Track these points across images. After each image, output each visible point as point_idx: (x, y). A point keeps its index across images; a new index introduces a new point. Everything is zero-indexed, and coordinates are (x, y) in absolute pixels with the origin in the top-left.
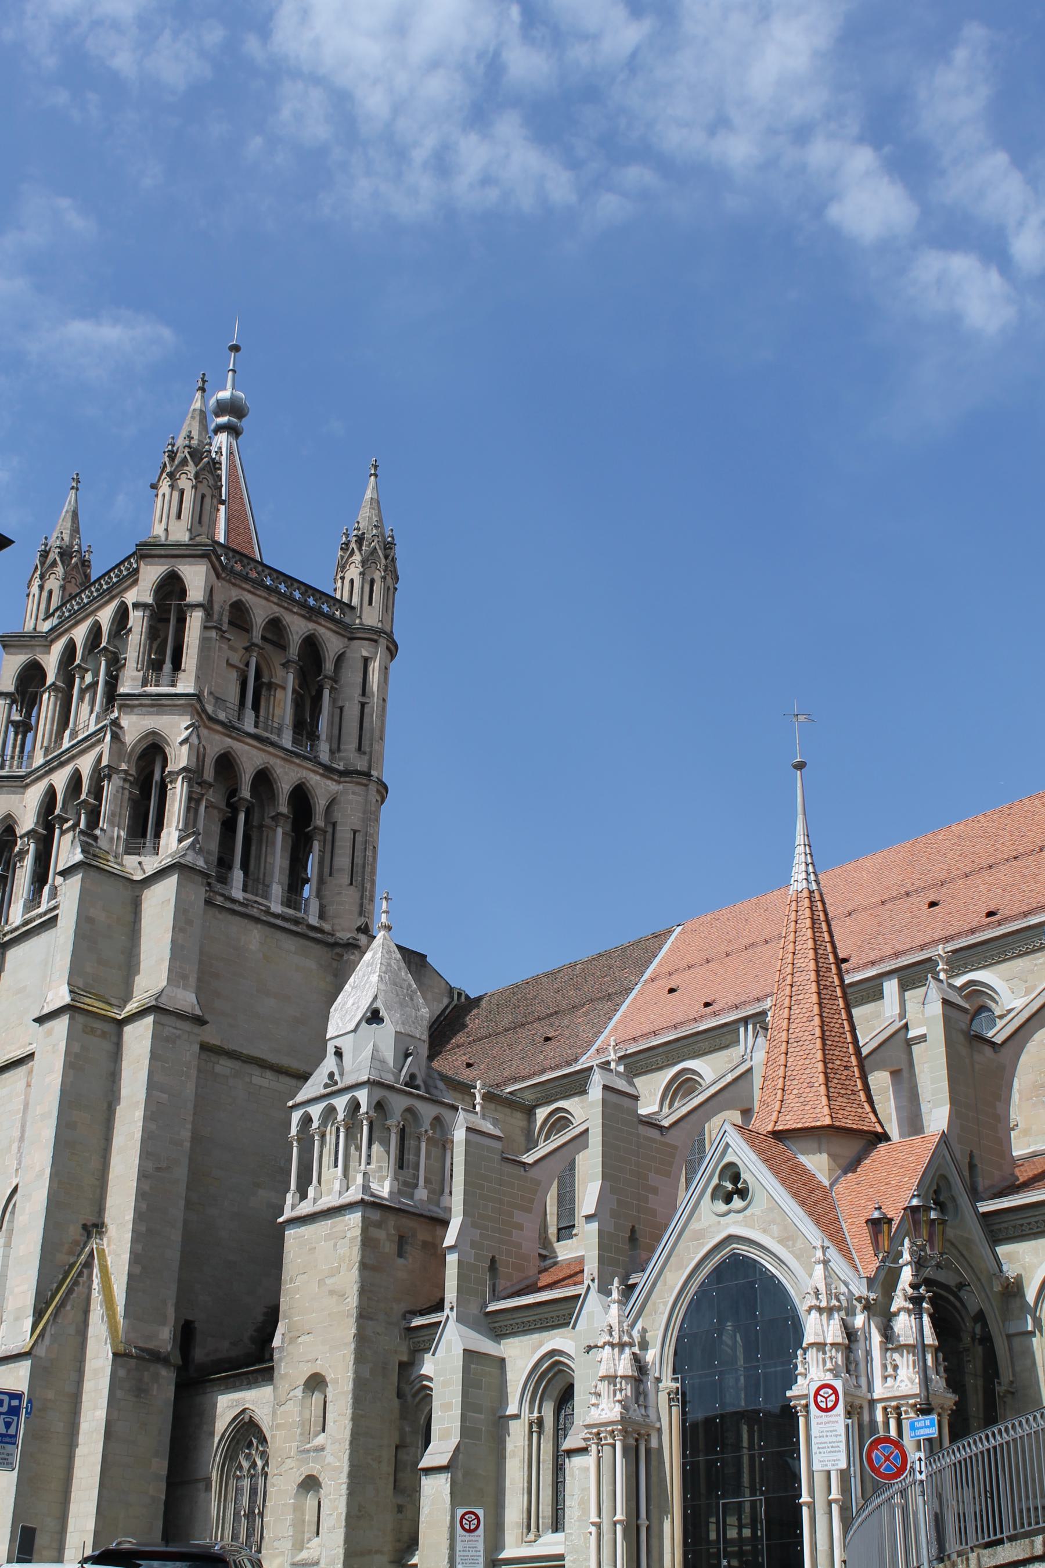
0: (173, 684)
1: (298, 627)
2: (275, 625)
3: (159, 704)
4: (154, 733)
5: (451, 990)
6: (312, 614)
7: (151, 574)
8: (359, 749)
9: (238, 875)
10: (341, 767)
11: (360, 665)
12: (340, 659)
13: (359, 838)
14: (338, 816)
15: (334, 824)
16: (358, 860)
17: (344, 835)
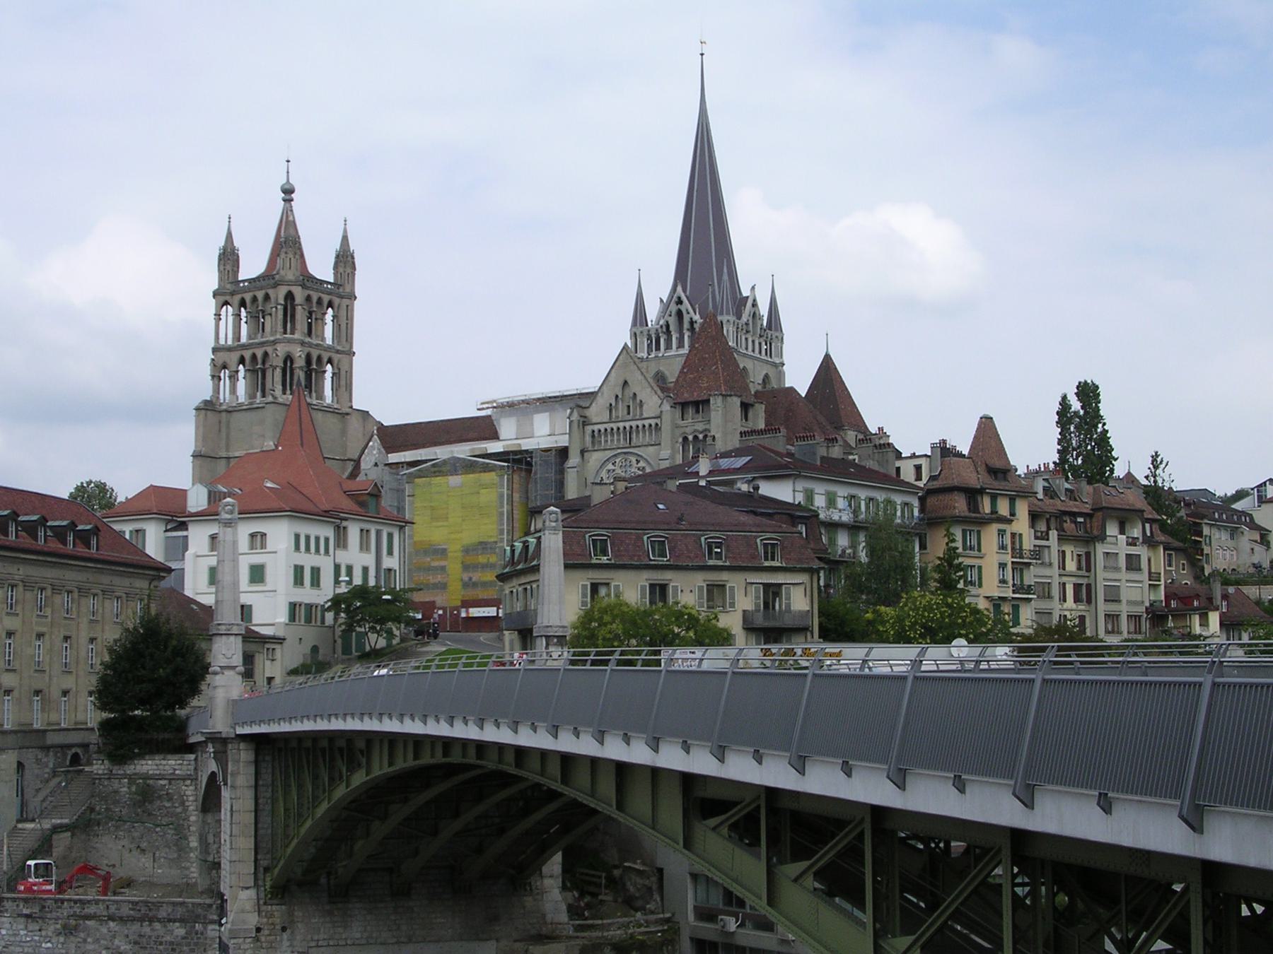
0: (292, 333)
1: (326, 298)
2: (320, 301)
3: (289, 341)
4: (289, 352)
5: (377, 422)
6: (329, 294)
7: (283, 291)
8: (347, 340)
9: (314, 394)
10: (339, 348)
11: (345, 307)
12: (339, 306)
13: (348, 374)
14: (340, 366)
15: (339, 369)
16: (348, 382)
17: (343, 373)
